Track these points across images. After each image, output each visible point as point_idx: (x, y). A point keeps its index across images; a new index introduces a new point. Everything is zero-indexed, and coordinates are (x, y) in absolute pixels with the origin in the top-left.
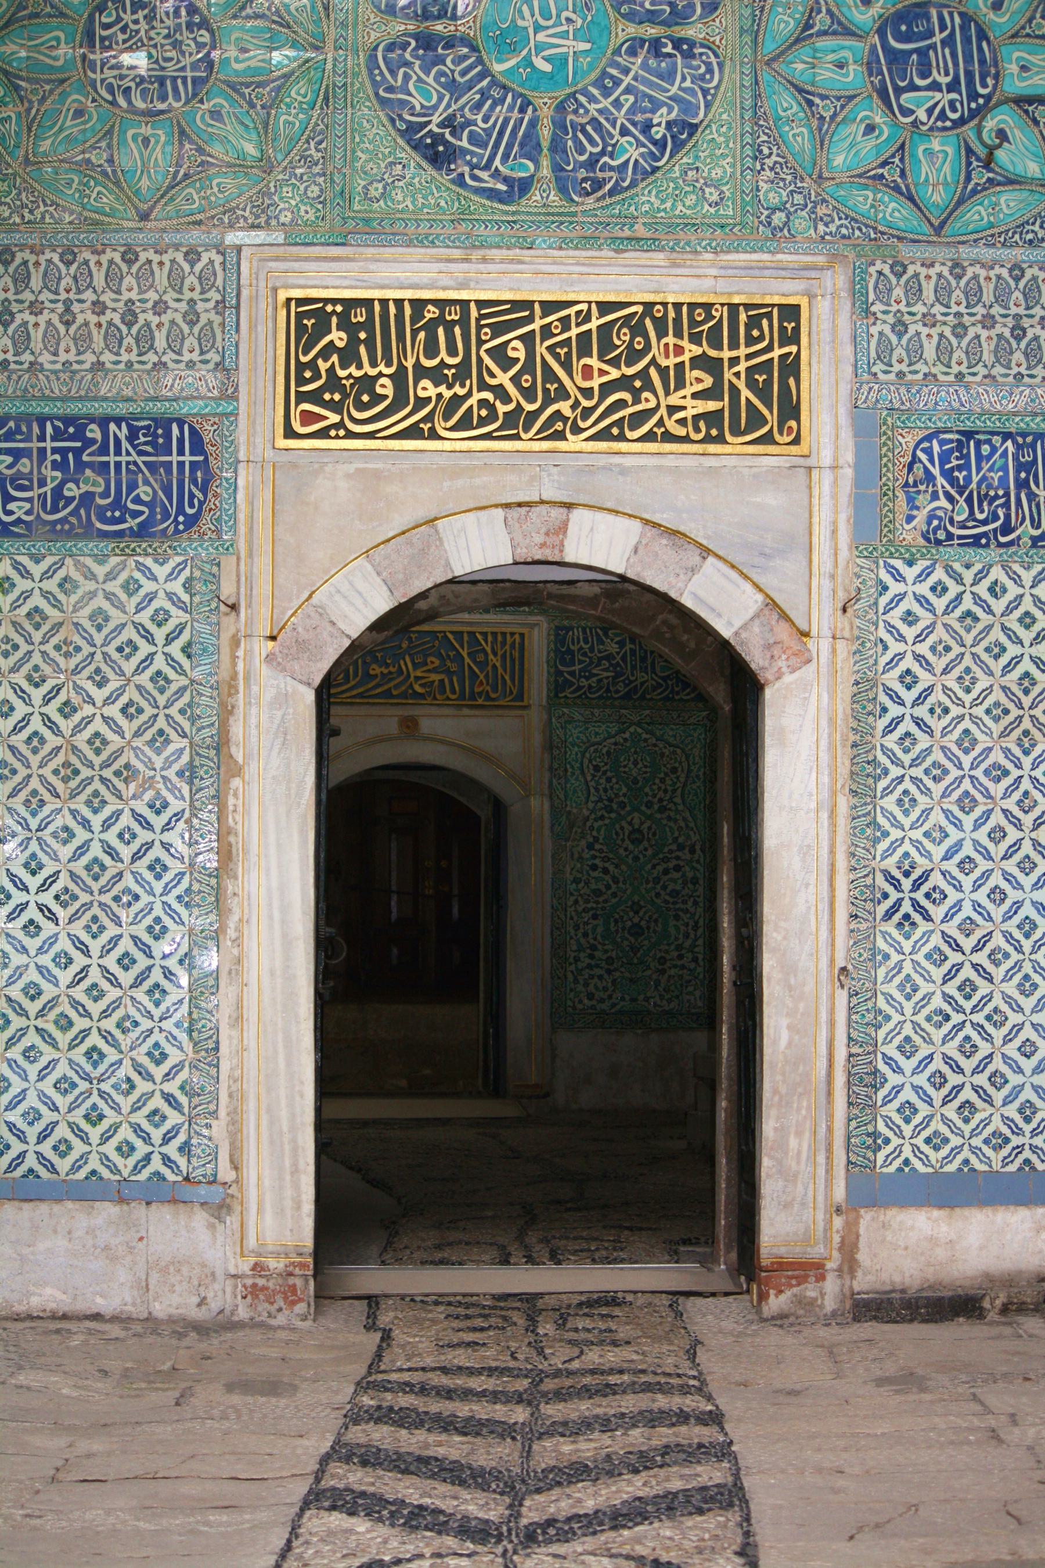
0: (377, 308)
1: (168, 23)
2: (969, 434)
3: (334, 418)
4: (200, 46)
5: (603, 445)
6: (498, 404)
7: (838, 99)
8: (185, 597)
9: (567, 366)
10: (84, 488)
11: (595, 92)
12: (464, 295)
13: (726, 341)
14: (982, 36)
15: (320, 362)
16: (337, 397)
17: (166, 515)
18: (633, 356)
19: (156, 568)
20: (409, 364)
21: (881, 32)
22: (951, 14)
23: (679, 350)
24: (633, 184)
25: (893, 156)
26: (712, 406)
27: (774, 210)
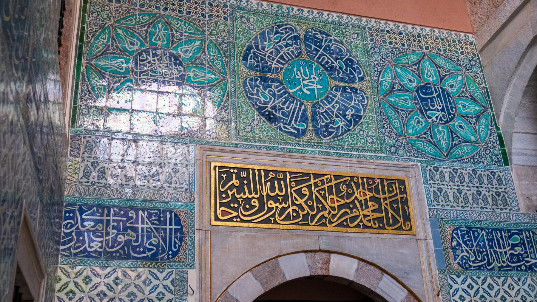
0: (251, 172)
1: (167, 62)
2: (470, 228)
3: (235, 214)
4: (179, 72)
5: (341, 229)
6: (300, 211)
7: (407, 111)
8: (172, 288)
9: (325, 198)
10: (127, 238)
11: (326, 102)
12: (284, 169)
13: (381, 192)
14: (449, 95)
15: (229, 191)
16: (236, 205)
17: (164, 251)
18: (349, 195)
19: (159, 274)
20: (265, 194)
21: (417, 91)
22: (438, 88)
23: (365, 194)
24: (342, 135)
25: (427, 131)
26: (378, 215)
27: (391, 146)
